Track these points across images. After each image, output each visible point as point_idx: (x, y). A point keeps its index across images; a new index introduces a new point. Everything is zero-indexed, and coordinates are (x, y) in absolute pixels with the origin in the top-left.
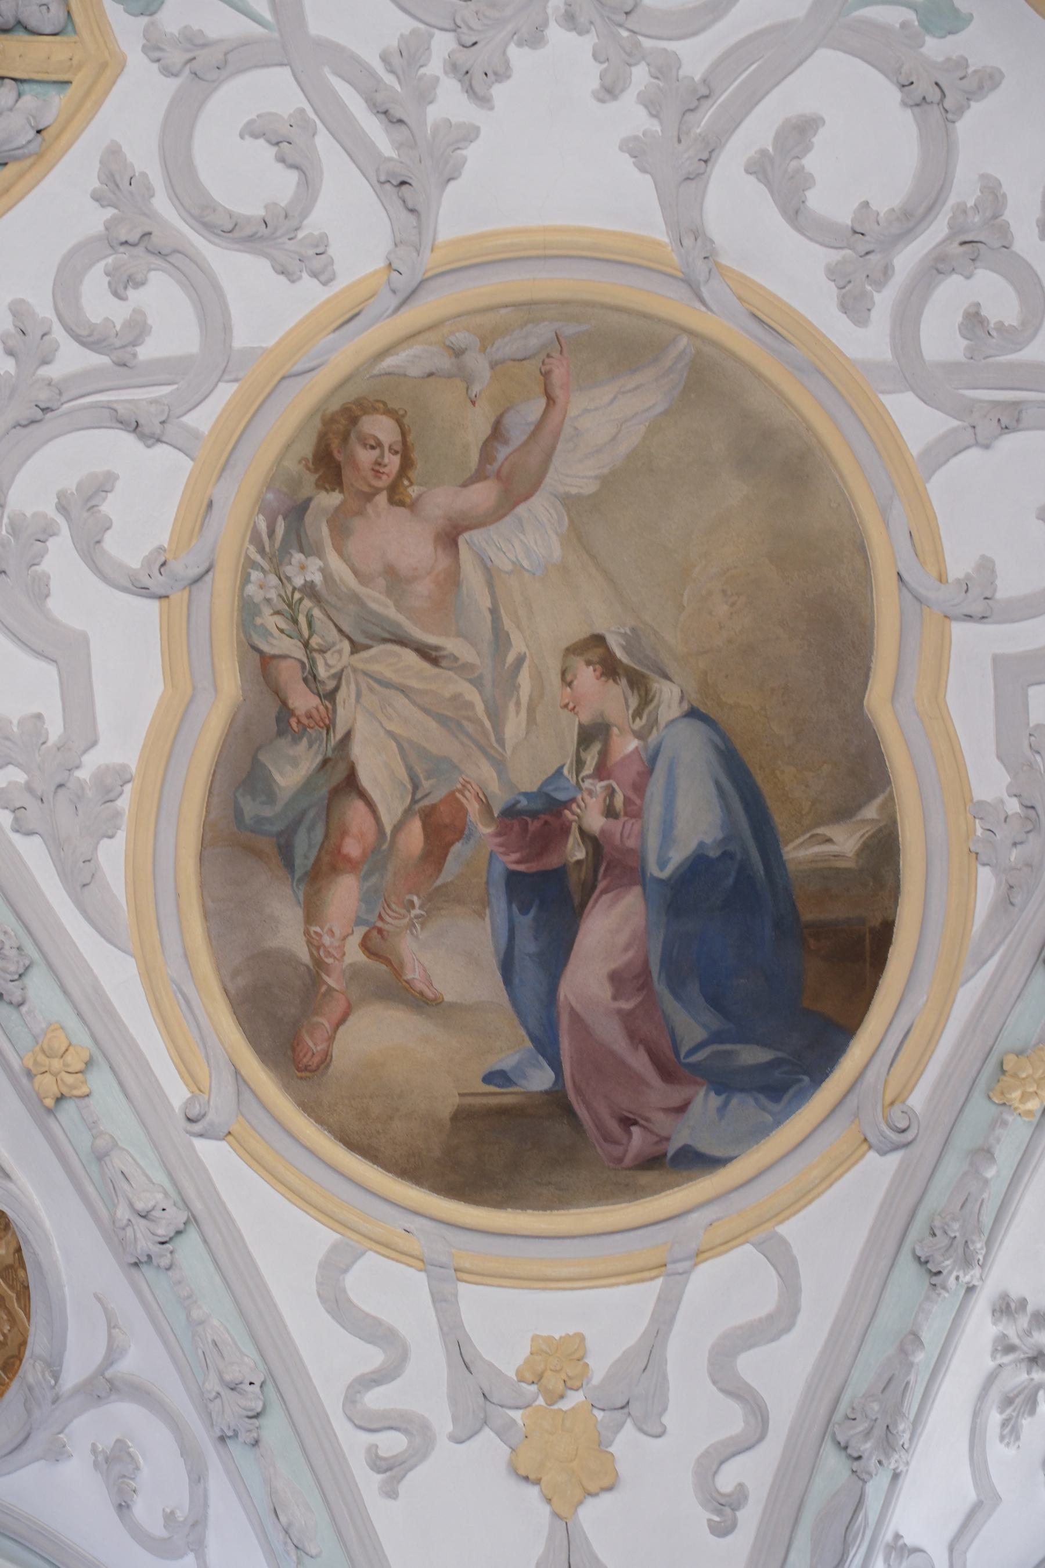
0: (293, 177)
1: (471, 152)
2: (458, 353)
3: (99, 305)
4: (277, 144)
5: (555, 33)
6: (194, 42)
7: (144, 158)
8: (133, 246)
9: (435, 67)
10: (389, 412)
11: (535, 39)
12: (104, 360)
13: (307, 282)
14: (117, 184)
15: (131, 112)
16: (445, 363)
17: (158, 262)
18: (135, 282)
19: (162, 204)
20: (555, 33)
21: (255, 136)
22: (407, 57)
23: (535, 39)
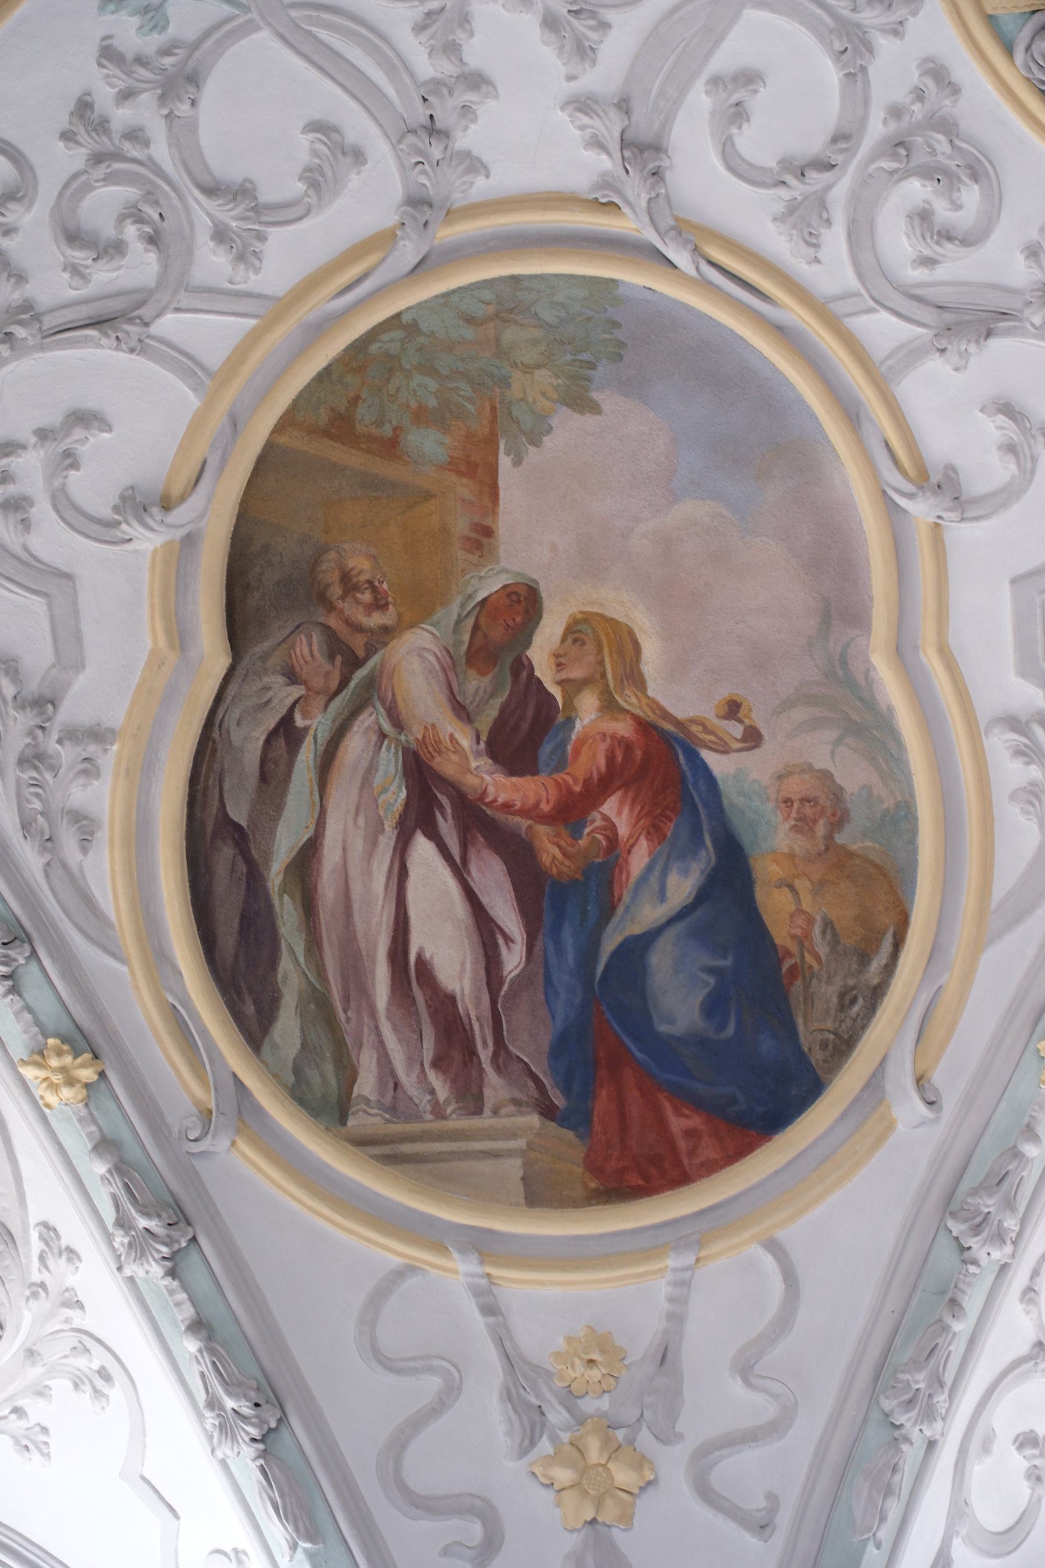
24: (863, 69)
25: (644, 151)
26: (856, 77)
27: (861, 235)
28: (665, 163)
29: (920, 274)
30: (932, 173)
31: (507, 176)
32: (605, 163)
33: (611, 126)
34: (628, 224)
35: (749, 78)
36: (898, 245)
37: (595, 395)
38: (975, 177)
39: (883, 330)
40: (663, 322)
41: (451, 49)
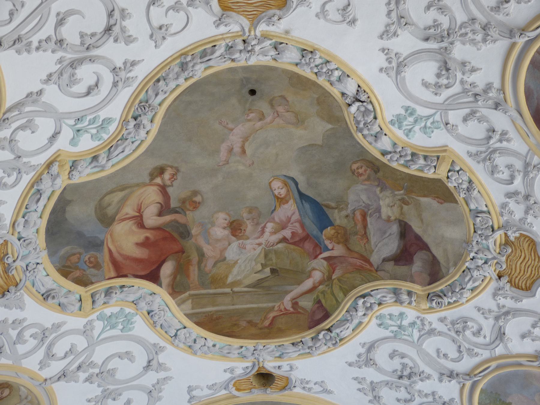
0: (63, 355)
1: (73, 383)
2: (26, 398)
3: (27, 334)
4: (70, 350)
5: (101, 389)
6: (92, 329)
7: (63, 329)
8: (43, 335)
9: (91, 371)
10: (10, 393)
11: (99, 386)
12: (15, 339)
13: (39, 367)
14: (57, 326)
15: (75, 322)
16: (23, 397)
17: (40, 340)
18: (35, 338)
19: (54, 335)
20: (101, 389)
21: (72, 346)
22: (92, 365)
23: (99, 386)
24: (439, 332)
25: (452, 375)
26: (440, 334)
27: (477, 345)
28: (455, 372)
29: (488, 339)
30: (465, 328)
31: (456, 395)
32: (454, 382)
33: (445, 379)
34: (468, 384)
35: (438, 351)
36: (480, 340)
37: (507, 402)
38: (466, 322)
39: (499, 350)
40: (491, 384)
41: (426, 395)
